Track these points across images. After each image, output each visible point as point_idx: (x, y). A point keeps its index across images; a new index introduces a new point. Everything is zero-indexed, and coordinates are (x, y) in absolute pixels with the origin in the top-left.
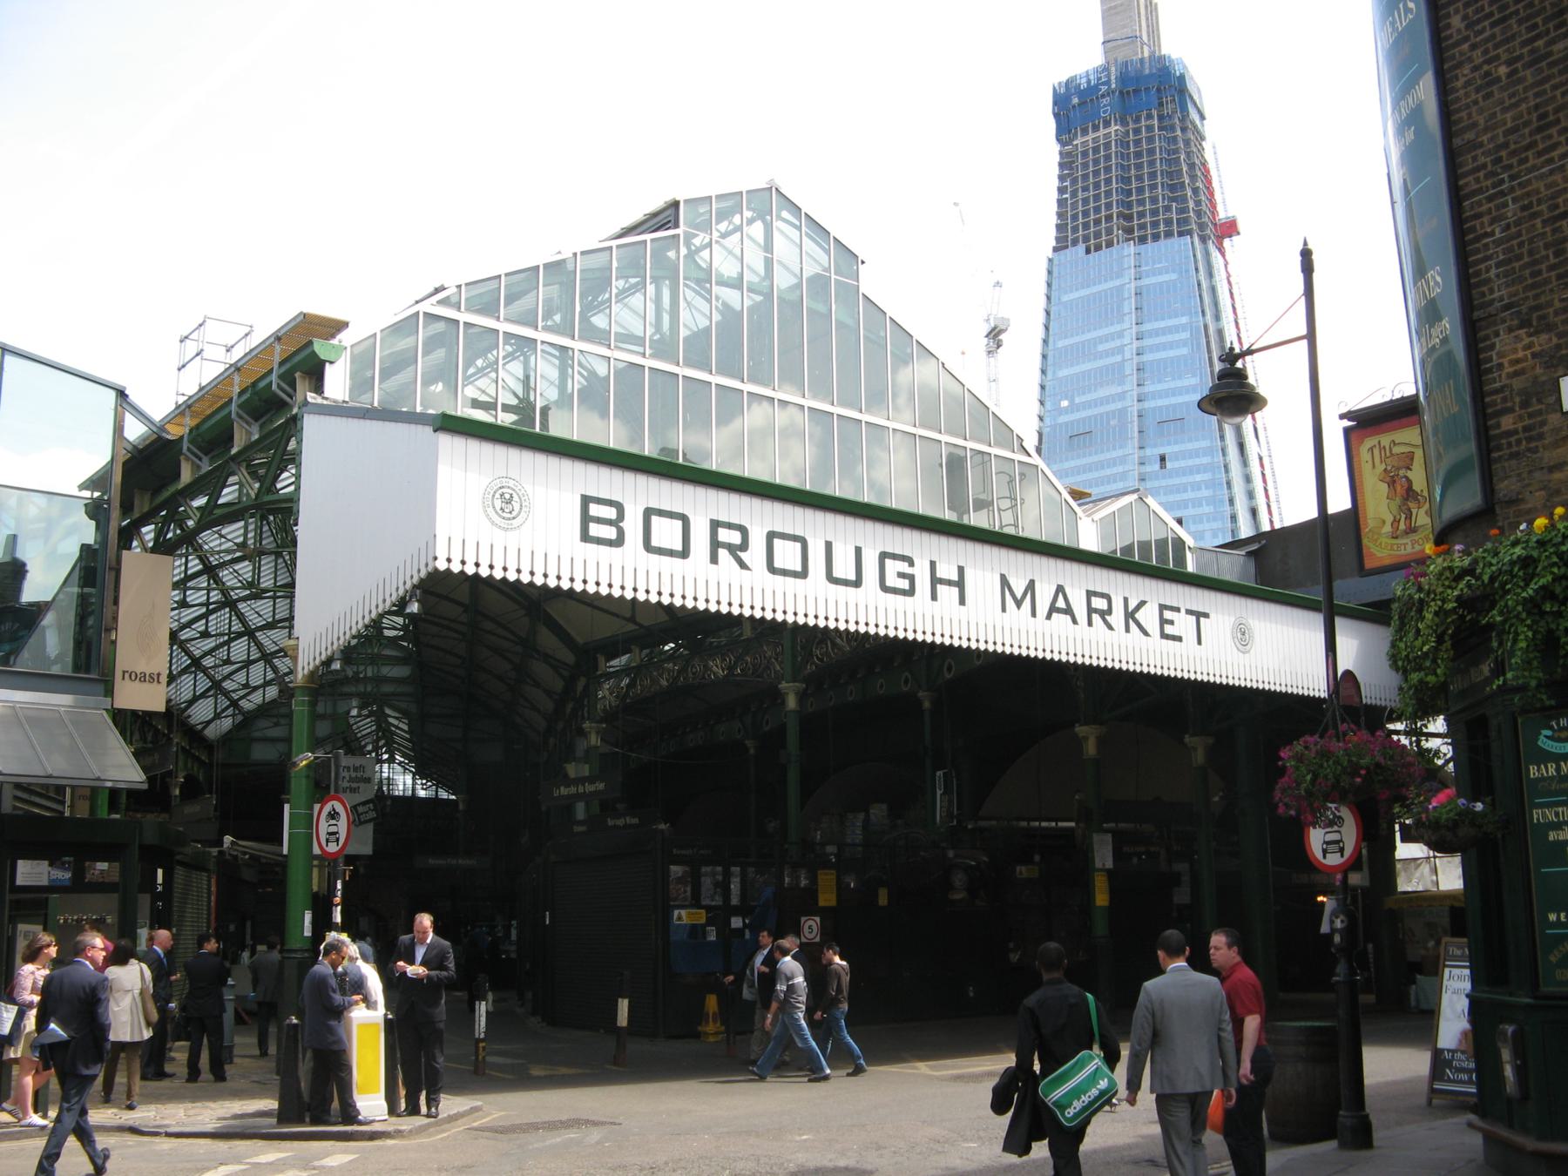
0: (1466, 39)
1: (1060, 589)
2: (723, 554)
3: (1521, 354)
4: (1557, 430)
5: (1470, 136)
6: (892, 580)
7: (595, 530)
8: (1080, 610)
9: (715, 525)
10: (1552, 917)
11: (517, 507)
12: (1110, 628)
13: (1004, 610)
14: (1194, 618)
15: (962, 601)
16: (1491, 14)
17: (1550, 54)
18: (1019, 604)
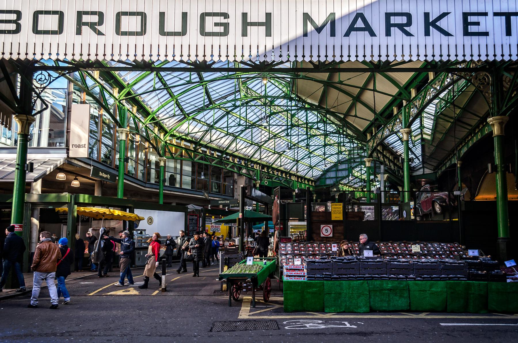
2: (85, 29)
6: (209, 27)
18: (319, 30)
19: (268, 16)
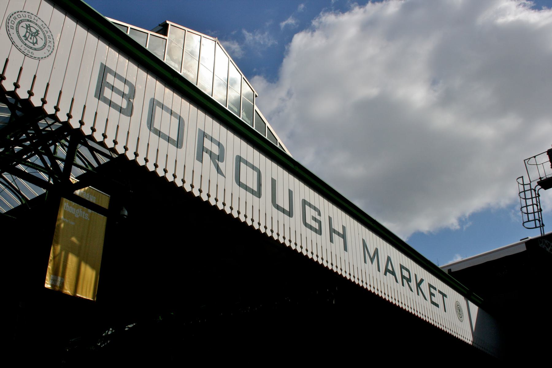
1: (389, 259)
11: (41, 43)
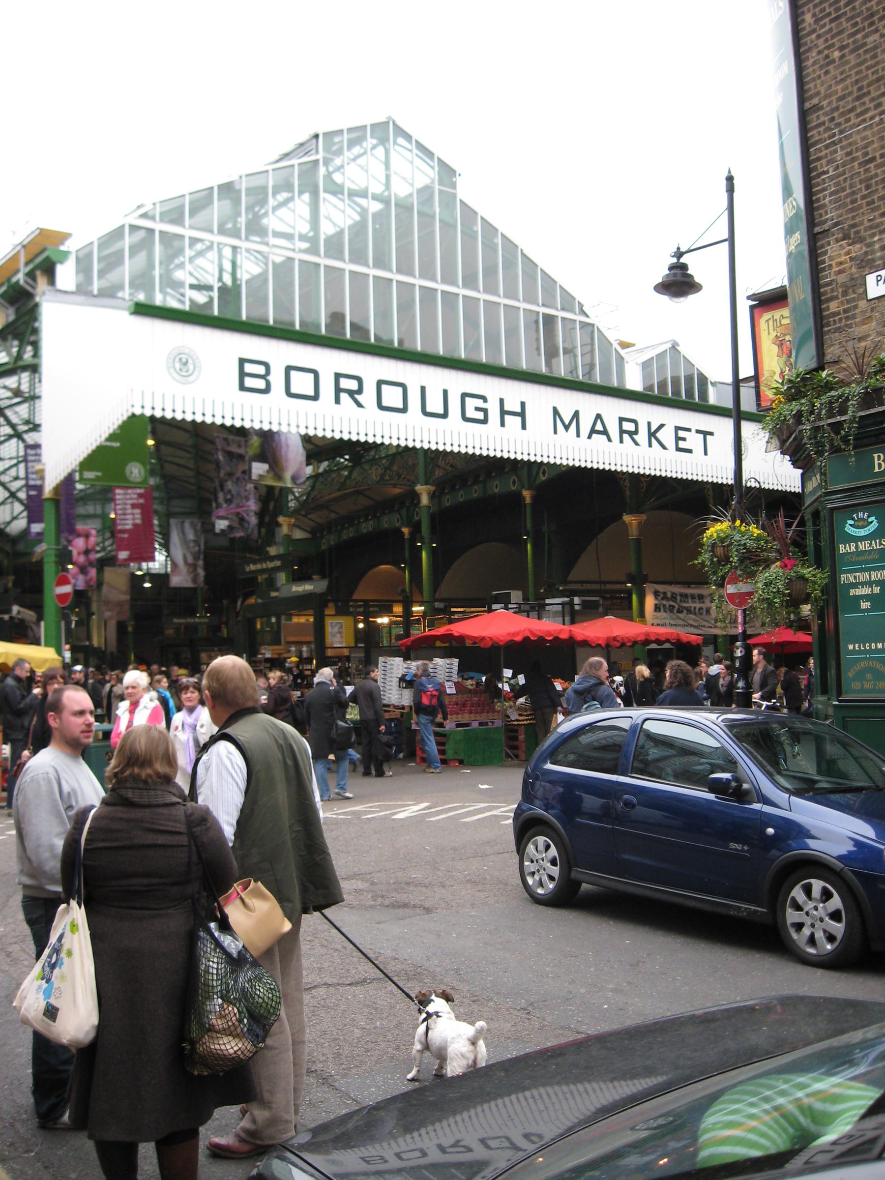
0: (814, 31)
1: (598, 417)
2: (344, 397)
3: (843, 259)
4: (864, 312)
5: (815, 101)
6: (471, 413)
7: (249, 382)
8: (614, 432)
9: (338, 376)
10: (851, 647)
12: (637, 444)
13: (555, 432)
14: (702, 436)
15: (524, 427)
16: (829, 14)
17: (865, 44)
18: (567, 427)
19: (523, 405)
